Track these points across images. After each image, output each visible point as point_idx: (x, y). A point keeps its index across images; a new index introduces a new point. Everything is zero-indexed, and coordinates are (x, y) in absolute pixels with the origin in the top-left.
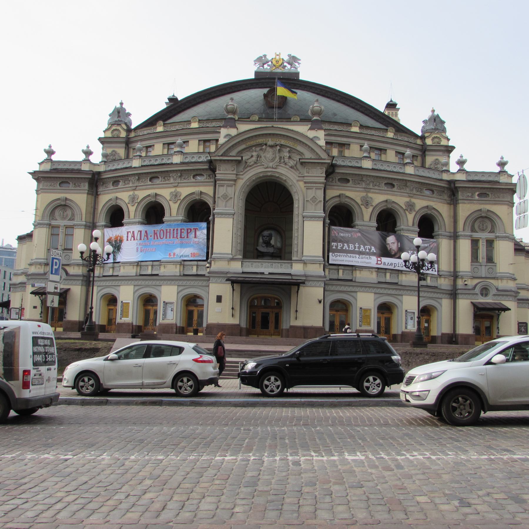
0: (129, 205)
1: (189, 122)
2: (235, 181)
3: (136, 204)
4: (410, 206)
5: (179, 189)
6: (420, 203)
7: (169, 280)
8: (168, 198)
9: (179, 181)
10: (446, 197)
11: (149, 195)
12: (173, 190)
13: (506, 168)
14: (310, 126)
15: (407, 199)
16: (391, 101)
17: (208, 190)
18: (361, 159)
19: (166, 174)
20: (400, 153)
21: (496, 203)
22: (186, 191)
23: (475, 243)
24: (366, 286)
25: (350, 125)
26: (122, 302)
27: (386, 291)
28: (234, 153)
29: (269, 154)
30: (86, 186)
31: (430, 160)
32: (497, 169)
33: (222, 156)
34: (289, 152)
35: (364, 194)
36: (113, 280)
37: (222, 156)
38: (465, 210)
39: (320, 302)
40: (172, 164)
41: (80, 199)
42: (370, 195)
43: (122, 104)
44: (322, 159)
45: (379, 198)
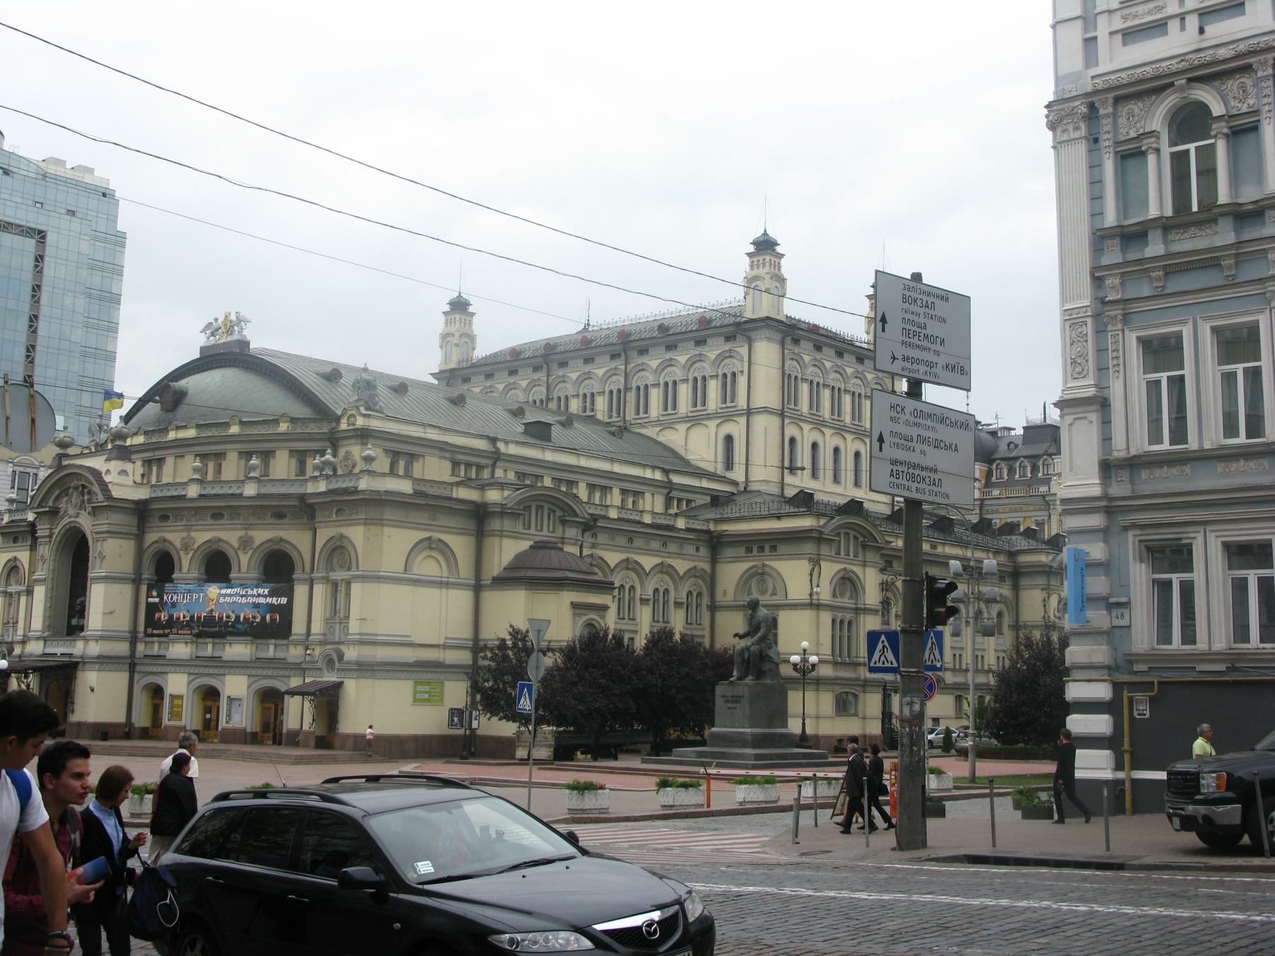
4: (245, 543)
6: (261, 536)
10: (305, 520)
14: (105, 457)
15: (242, 533)
18: (186, 484)
20: (298, 451)
21: (353, 523)
23: (335, 585)
24: (178, 664)
25: (227, 425)
27: (201, 670)
28: (50, 504)
31: (342, 452)
33: (40, 506)
34: (89, 493)
35: (185, 534)
37: (40, 506)
39: (92, 690)
42: (193, 534)
45: (202, 537)
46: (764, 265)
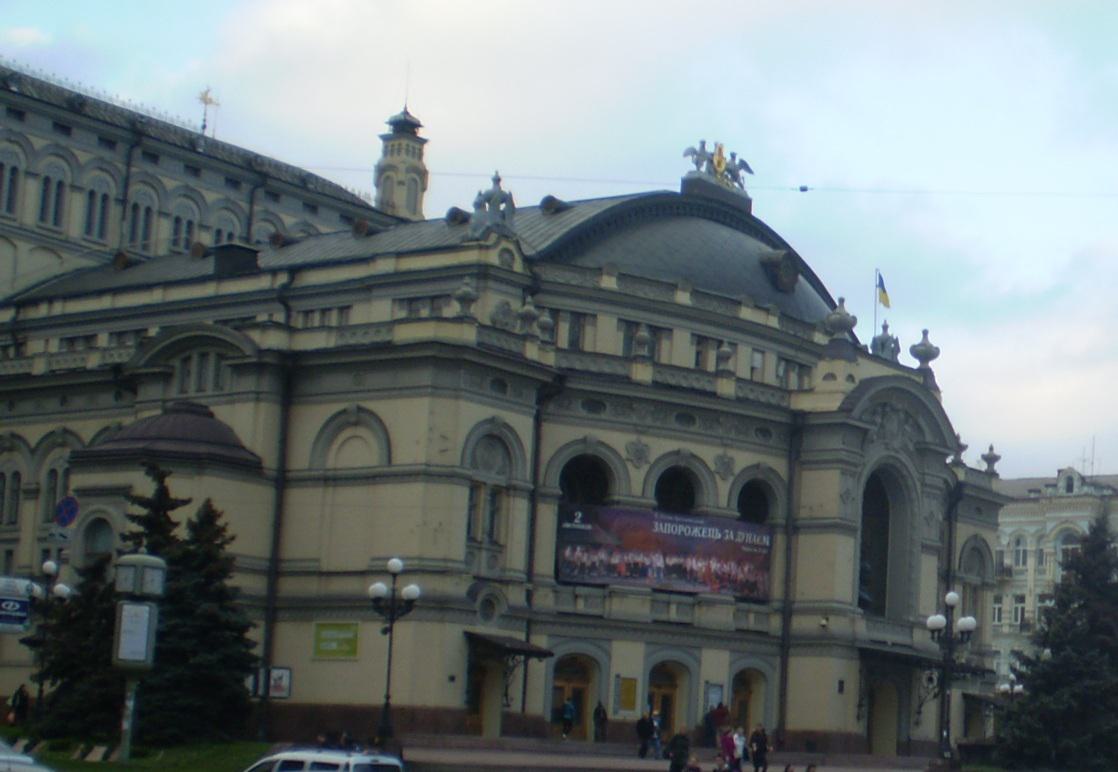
0: (630, 466)
1: (673, 287)
2: (856, 466)
3: (646, 468)
5: (731, 453)
7: (717, 638)
8: (713, 467)
9: (733, 435)
11: (677, 453)
12: (719, 451)
13: (997, 467)
16: (406, 113)
17: (779, 465)
19: (713, 417)
22: (743, 459)
26: (618, 676)
29: (892, 426)
30: (533, 401)
32: (984, 467)
36: (595, 627)
38: (963, 532)
40: (713, 395)
41: (522, 424)
43: (497, 180)
44: (946, 446)
46: (399, 151)
